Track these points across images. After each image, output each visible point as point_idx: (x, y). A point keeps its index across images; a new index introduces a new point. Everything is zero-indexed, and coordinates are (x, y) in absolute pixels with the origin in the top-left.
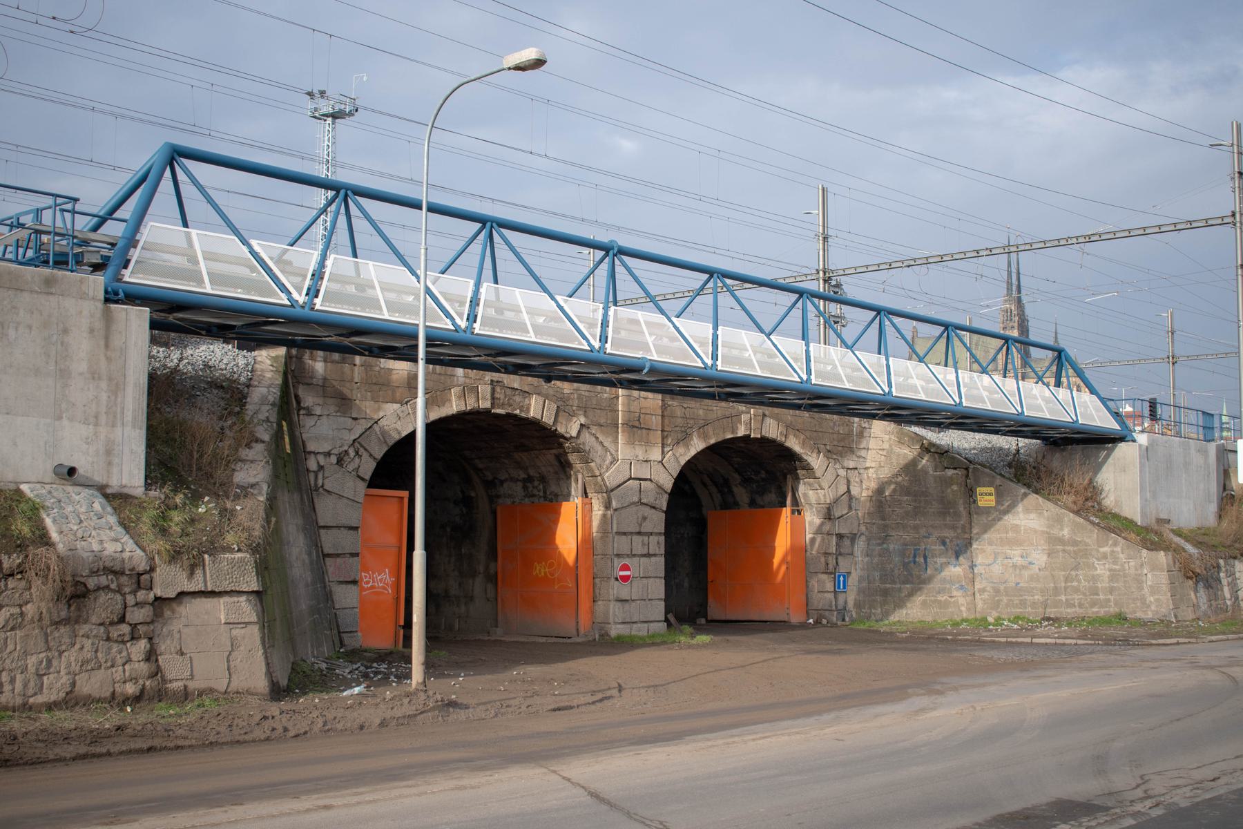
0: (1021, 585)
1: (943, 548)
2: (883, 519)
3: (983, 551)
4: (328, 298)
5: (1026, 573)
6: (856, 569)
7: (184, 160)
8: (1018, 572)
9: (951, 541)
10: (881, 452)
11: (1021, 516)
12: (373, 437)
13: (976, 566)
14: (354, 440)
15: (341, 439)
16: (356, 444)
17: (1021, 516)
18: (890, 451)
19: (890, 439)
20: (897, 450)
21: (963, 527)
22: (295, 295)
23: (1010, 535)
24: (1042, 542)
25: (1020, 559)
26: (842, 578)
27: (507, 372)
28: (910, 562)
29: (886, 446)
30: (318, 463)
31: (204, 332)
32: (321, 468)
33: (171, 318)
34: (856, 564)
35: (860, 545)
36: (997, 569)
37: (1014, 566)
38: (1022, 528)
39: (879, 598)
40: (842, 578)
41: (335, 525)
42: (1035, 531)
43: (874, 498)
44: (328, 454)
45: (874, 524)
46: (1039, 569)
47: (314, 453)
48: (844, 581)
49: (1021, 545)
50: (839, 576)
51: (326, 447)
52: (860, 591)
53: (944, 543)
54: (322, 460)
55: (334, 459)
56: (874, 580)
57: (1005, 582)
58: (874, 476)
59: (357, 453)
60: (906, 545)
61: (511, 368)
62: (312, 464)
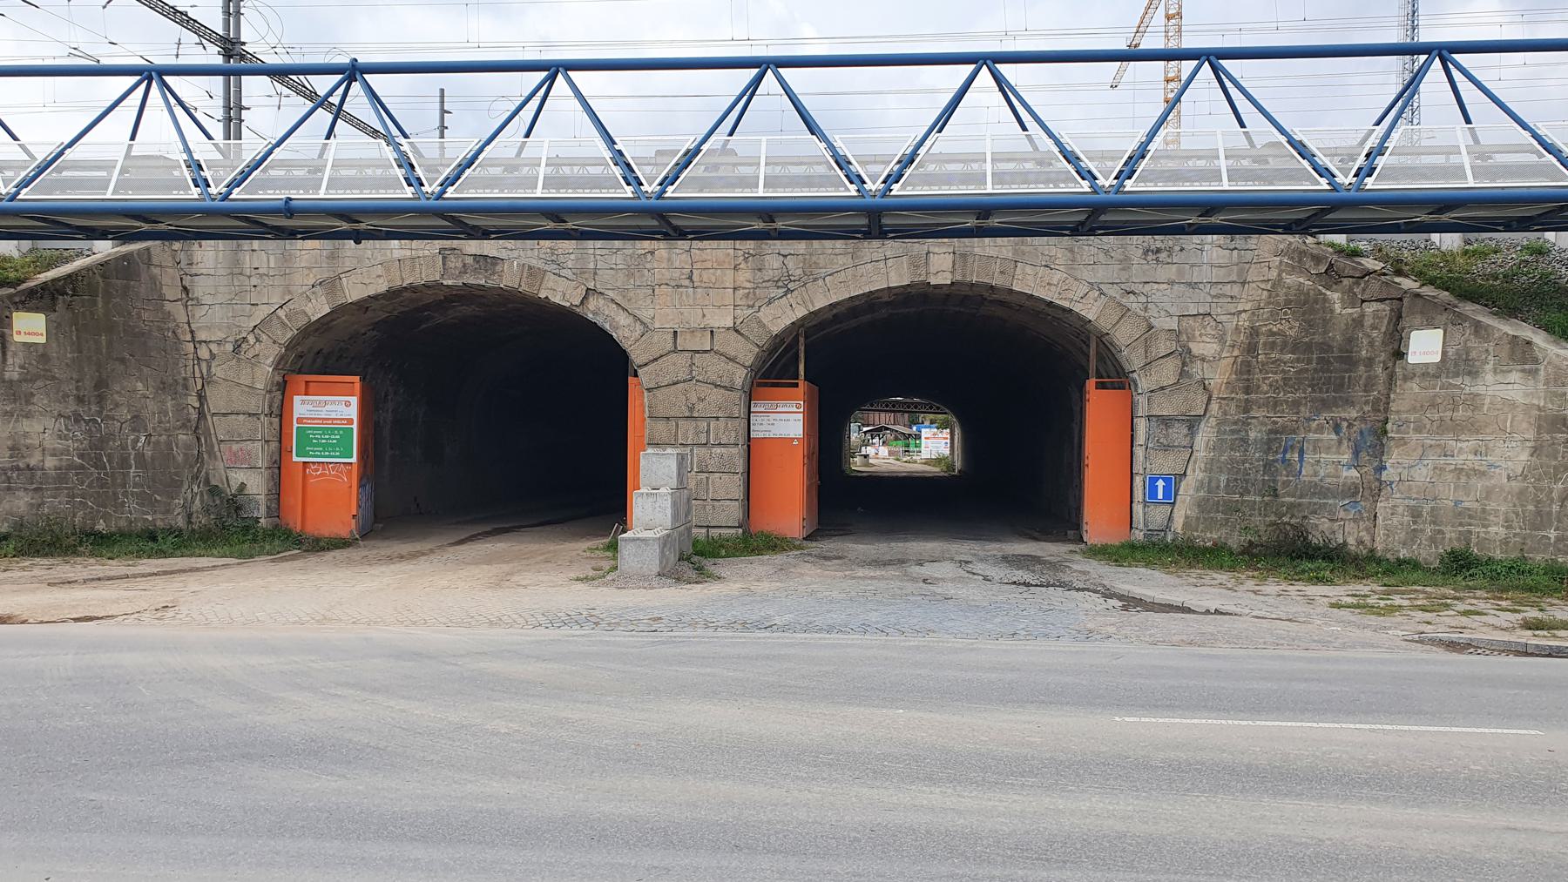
0: (1466, 505)
1: (1334, 436)
2: (1247, 391)
3: (1403, 442)
4: (1389, 173)
5: (1479, 485)
6: (1194, 471)
7: (1455, 56)
8: (1463, 479)
9: (1350, 426)
10: (1263, 286)
11: (1489, 378)
12: (275, 321)
13: (1385, 469)
14: (255, 327)
15: (239, 326)
16: (256, 331)
17: (1489, 378)
18: (1278, 282)
19: (1281, 262)
20: (1290, 279)
21: (1377, 400)
22: (1340, 179)
23: (1460, 414)
24: (1525, 425)
25: (1471, 457)
26: (1160, 484)
27: (1508, 228)
28: (1277, 461)
29: (1274, 274)
30: (211, 351)
31: (1501, 228)
32: (213, 356)
33: (1216, 220)
34: (1195, 462)
35: (1205, 435)
36: (1422, 474)
37: (1459, 471)
38: (1487, 401)
39: (1220, 516)
40: (1160, 484)
41: (229, 412)
42: (1513, 405)
43: (1239, 360)
44: (219, 343)
45: (1233, 399)
46: (1509, 478)
47: (205, 342)
48: (1166, 489)
49: (1478, 432)
50: (1154, 480)
51: (220, 335)
52: (1202, 505)
53: (1337, 429)
54: (213, 347)
55: (230, 347)
56: (1218, 487)
57: (1435, 499)
58: (1247, 324)
59: (258, 340)
60: (1276, 432)
61: (1515, 224)
62: (204, 353)
